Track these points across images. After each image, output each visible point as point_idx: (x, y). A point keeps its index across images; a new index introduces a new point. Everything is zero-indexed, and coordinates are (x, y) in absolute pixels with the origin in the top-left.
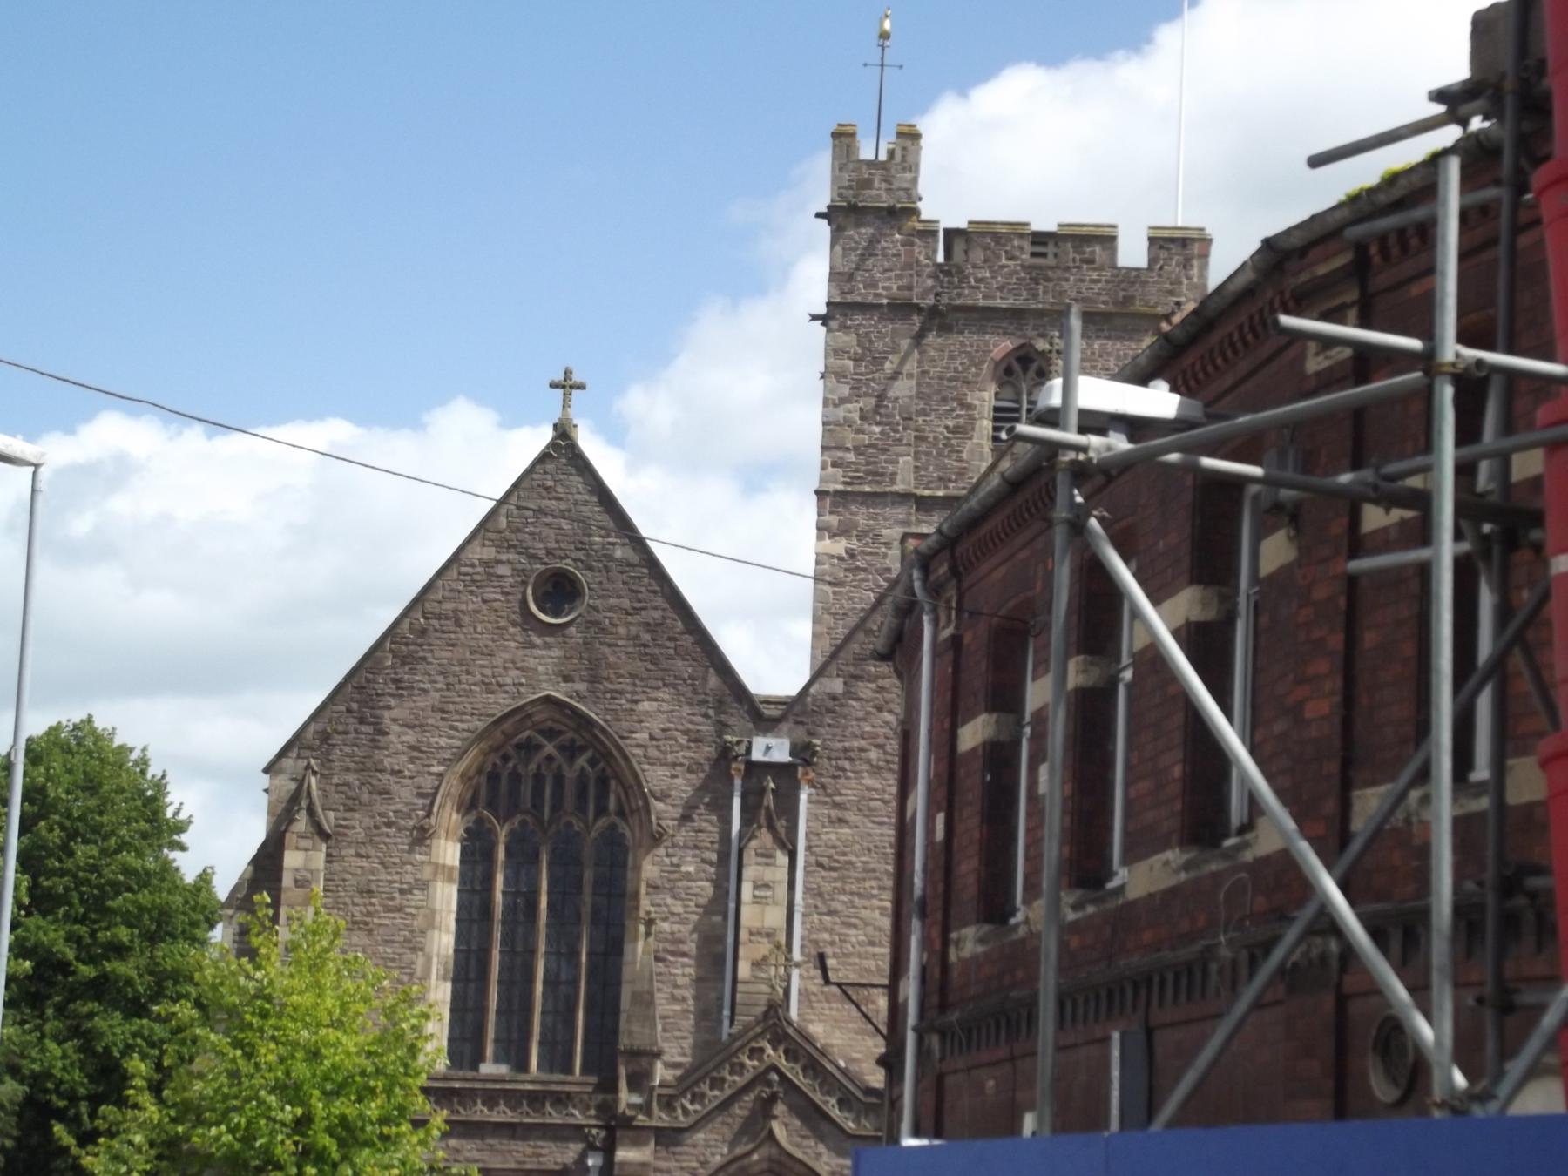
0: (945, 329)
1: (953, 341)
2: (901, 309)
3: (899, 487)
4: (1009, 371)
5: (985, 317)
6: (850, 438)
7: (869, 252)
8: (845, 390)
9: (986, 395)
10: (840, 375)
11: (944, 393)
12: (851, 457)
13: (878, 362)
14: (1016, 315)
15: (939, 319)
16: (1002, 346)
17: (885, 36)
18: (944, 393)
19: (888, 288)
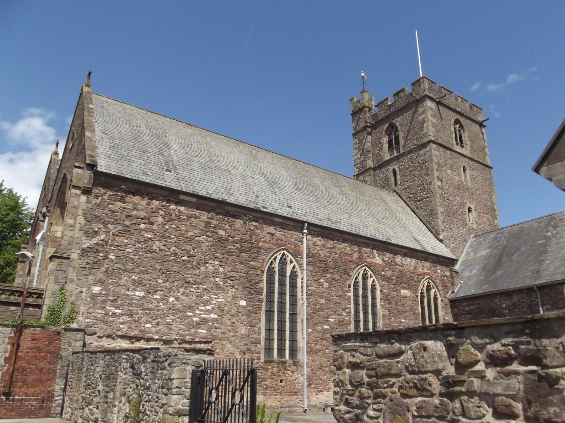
0: (375, 129)
1: (377, 130)
2: (365, 128)
3: (368, 167)
4: (390, 131)
5: (382, 121)
6: (358, 161)
7: (359, 120)
8: (357, 151)
9: (385, 139)
10: (356, 149)
11: (377, 143)
12: (359, 165)
13: (362, 142)
14: (387, 117)
15: (374, 127)
16: (386, 126)
17: (363, 77)
18: (377, 143)
19: (362, 125)
